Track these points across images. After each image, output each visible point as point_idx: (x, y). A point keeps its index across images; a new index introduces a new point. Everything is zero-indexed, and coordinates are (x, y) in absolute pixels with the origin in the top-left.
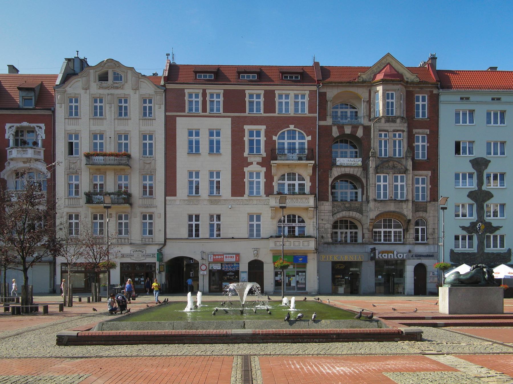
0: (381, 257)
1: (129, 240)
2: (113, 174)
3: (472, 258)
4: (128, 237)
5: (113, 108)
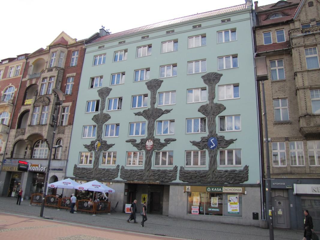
0: (31, 170)
3: (88, 172)
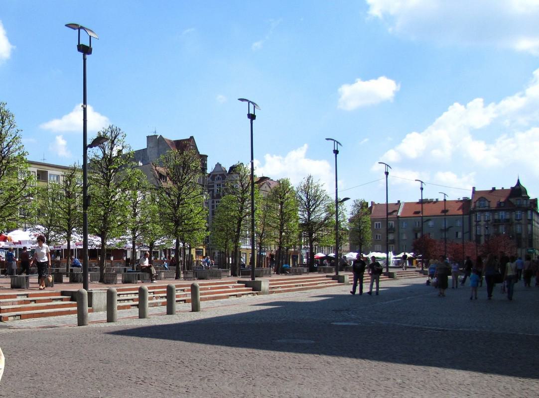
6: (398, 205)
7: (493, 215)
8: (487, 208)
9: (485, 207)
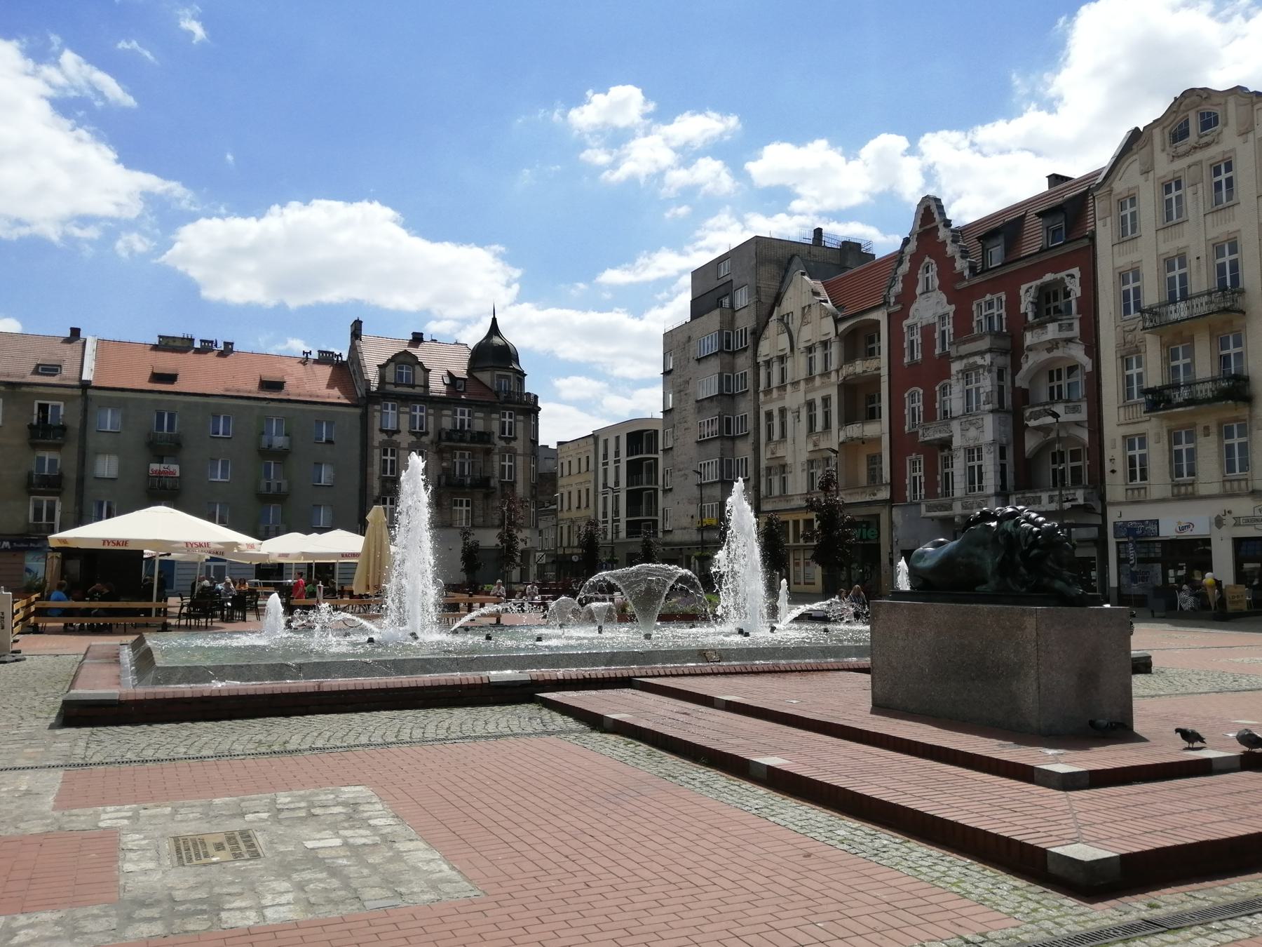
1: (1250, 483)
2: (1208, 338)
4: (1246, 477)
5: (1200, 192)
6: (77, 345)
7: (438, 418)
8: (419, 390)
9: (413, 386)
